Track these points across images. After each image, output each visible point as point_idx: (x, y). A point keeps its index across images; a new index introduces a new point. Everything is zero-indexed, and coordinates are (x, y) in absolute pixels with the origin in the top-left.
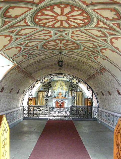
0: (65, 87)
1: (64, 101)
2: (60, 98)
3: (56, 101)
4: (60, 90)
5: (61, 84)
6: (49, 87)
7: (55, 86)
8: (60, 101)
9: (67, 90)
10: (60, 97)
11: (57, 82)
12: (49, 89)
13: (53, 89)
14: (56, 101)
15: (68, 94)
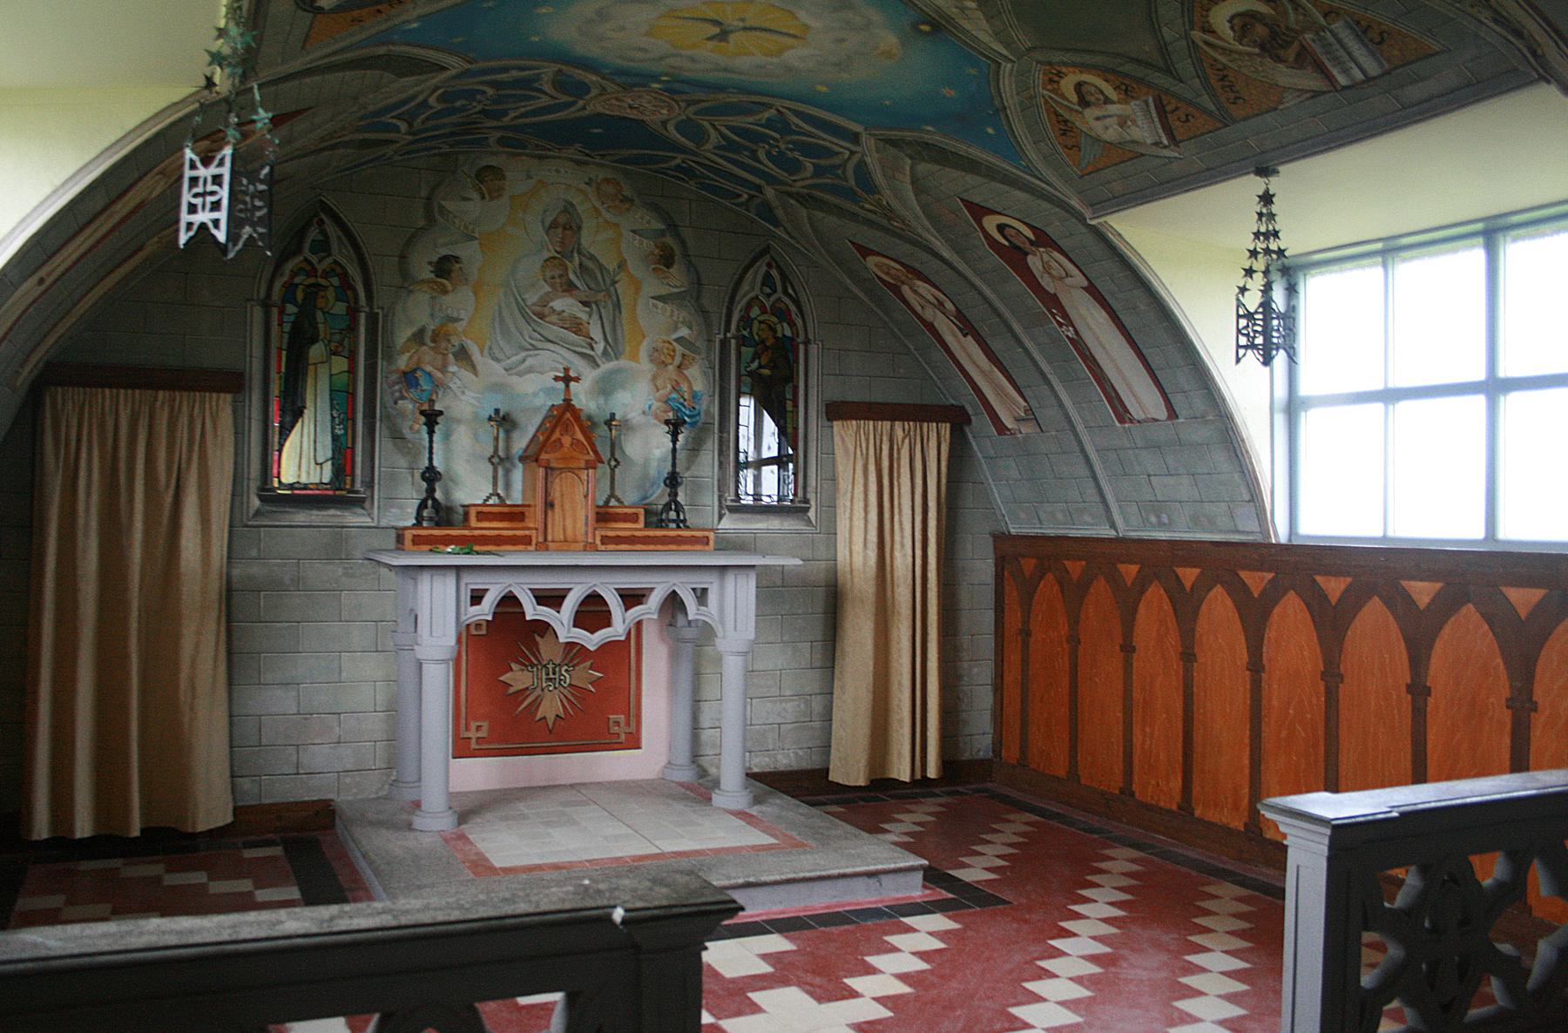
0: (664, 312)
1: (673, 603)
2: (566, 544)
3: (509, 600)
4: (553, 359)
5: (566, 226)
6: (314, 291)
7: (445, 267)
8: (593, 613)
9: (698, 379)
10: (574, 515)
11: (490, 181)
12: (300, 340)
13: (403, 335)
14: (509, 600)
15: (712, 445)
